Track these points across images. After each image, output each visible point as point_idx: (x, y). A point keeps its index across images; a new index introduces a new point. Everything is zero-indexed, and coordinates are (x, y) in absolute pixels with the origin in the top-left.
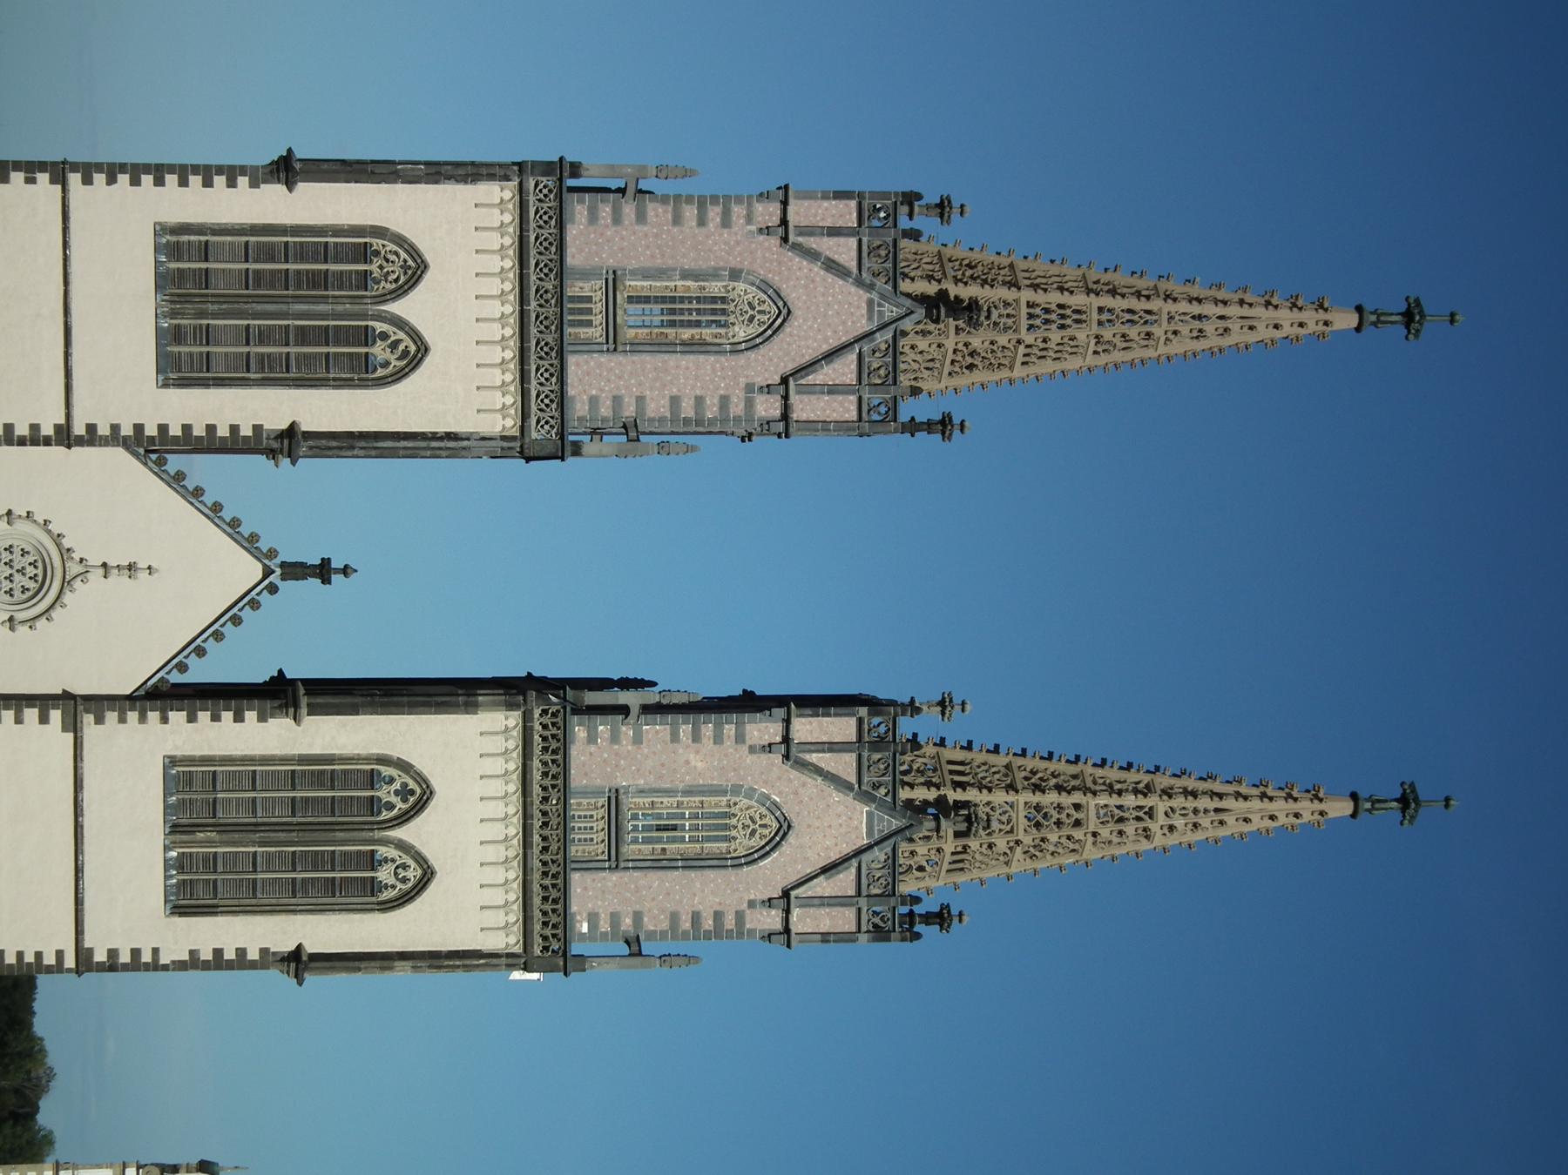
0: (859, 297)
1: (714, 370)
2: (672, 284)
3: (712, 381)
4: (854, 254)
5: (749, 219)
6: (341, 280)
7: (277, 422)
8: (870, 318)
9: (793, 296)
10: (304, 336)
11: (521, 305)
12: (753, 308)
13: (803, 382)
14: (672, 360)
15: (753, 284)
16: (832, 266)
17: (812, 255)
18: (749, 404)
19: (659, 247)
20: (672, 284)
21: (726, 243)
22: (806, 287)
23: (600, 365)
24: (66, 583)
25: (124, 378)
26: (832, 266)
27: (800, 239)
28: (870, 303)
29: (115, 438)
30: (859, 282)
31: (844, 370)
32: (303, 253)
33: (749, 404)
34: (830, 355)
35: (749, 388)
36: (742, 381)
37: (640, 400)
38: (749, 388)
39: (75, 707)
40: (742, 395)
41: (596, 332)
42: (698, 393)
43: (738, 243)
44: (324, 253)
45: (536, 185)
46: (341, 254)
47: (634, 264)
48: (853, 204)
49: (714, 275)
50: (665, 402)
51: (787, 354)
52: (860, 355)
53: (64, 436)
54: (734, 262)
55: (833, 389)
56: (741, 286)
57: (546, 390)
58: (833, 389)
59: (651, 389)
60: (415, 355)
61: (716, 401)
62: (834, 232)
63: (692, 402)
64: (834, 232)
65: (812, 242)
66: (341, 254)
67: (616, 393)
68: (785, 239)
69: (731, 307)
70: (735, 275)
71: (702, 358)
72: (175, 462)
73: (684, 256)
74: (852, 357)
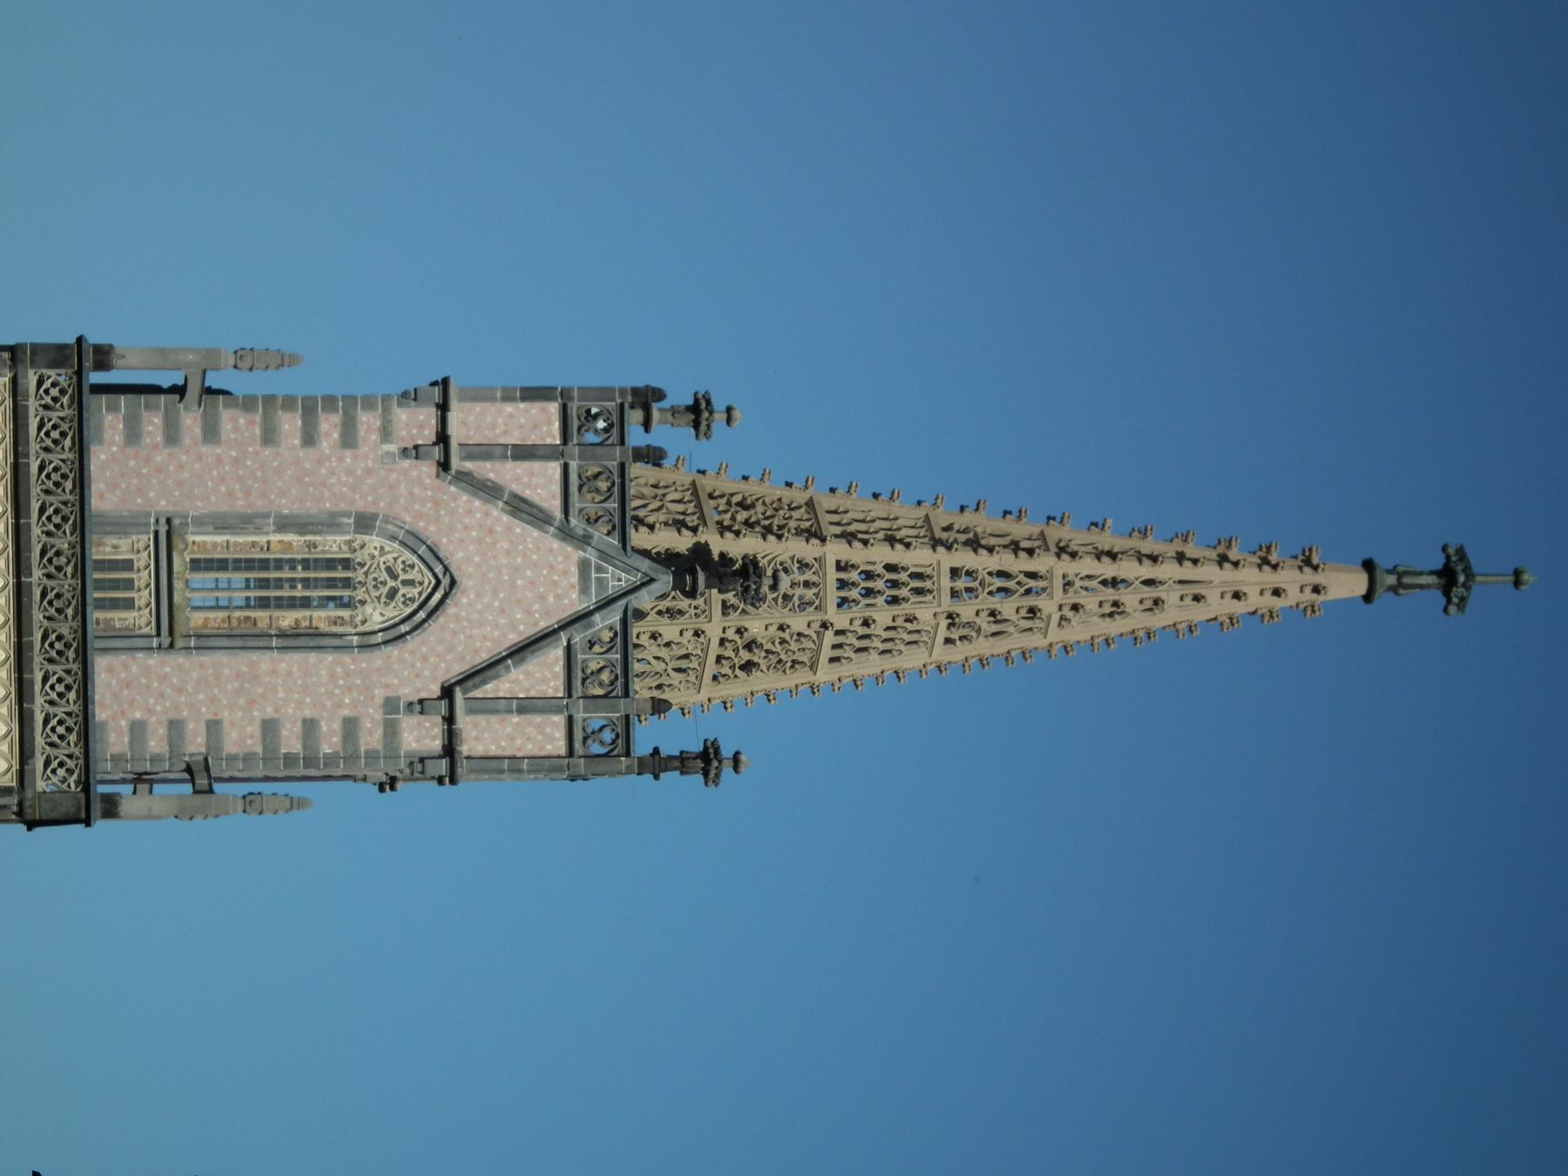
0: (567, 557)
1: (333, 676)
2: (262, 539)
3: (331, 695)
4: (556, 488)
5: (386, 434)
8: (584, 590)
11: (18, 573)
12: (394, 577)
13: (477, 693)
14: (265, 661)
15: (393, 538)
16: (520, 507)
17: (489, 491)
18: (391, 730)
19: (241, 480)
20: (262, 539)
21: (350, 472)
22: (480, 541)
23: (147, 671)
26: (520, 507)
27: (469, 465)
28: (584, 566)
30: (566, 534)
31: (543, 674)
33: (391, 730)
34: (521, 651)
35: (390, 705)
36: (379, 694)
37: (214, 727)
38: (390, 705)
40: (379, 716)
41: (140, 618)
42: (308, 713)
43: (369, 472)
45: (40, 383)
47: (199, 508)
48: (554, 408)
49: (331, 523)
50: (254, 729)
51: (451, 649)
52: (569, 650)
54: (362, 504)
55: (527, 706)
56: (374, 541)
57: (60, 711)
58: (527, 706)
59: (232, 707)
61: (337, 726)
62: (523, 453)
63: (298, 728)
64: (523, 453)
65: (488, 470)
67: (173, 715)
68: (444, 465)
69: (359, 576)
70: (365, 523)
71: (313, 657)
73: (282, 493)
74: (554, 655)
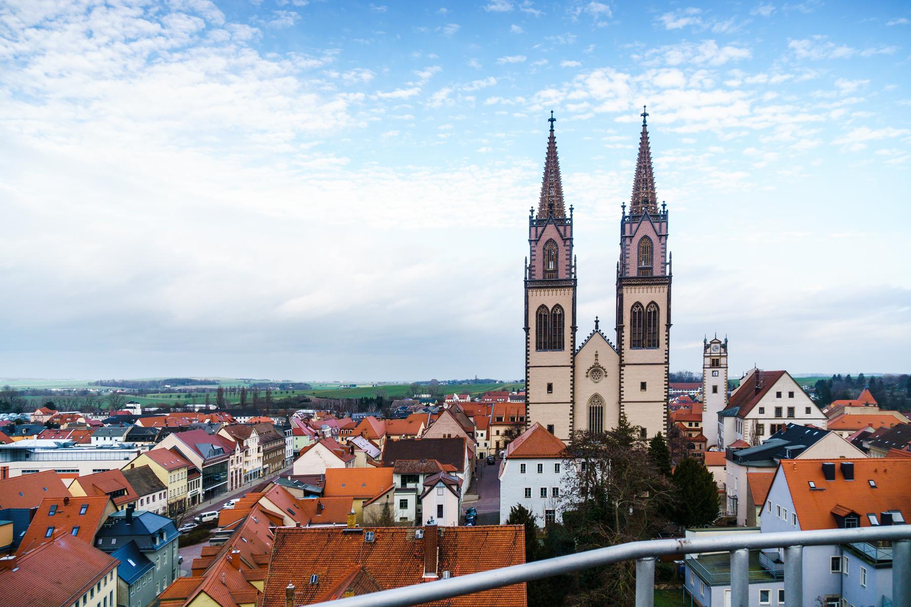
6: (545, 319)
7: (570, 331)
9: (547, 238)
10: (555, 326)
14: (559, 260)
16: (543, 232)
17: (541, 235)
24: (599, 366)
25: (563, 357)
26: (543, 232)
29: (573, 358)
31: (561, 229)
32: (541, 326)
34: (559, 231)
39: (622, 365)
44: (541, 323)
46: (541, 319)
53: (573, 367)
55: (565, 230)
58: (565, 230)
60: (558, 306)
66: (541, 319)
72: (577, 348)
